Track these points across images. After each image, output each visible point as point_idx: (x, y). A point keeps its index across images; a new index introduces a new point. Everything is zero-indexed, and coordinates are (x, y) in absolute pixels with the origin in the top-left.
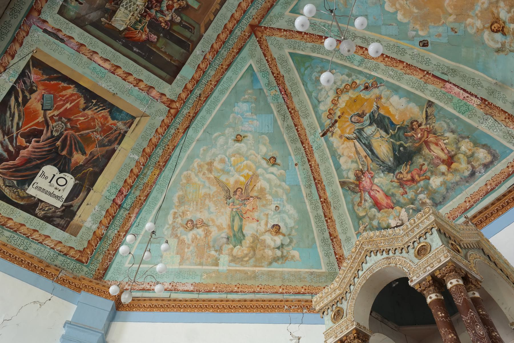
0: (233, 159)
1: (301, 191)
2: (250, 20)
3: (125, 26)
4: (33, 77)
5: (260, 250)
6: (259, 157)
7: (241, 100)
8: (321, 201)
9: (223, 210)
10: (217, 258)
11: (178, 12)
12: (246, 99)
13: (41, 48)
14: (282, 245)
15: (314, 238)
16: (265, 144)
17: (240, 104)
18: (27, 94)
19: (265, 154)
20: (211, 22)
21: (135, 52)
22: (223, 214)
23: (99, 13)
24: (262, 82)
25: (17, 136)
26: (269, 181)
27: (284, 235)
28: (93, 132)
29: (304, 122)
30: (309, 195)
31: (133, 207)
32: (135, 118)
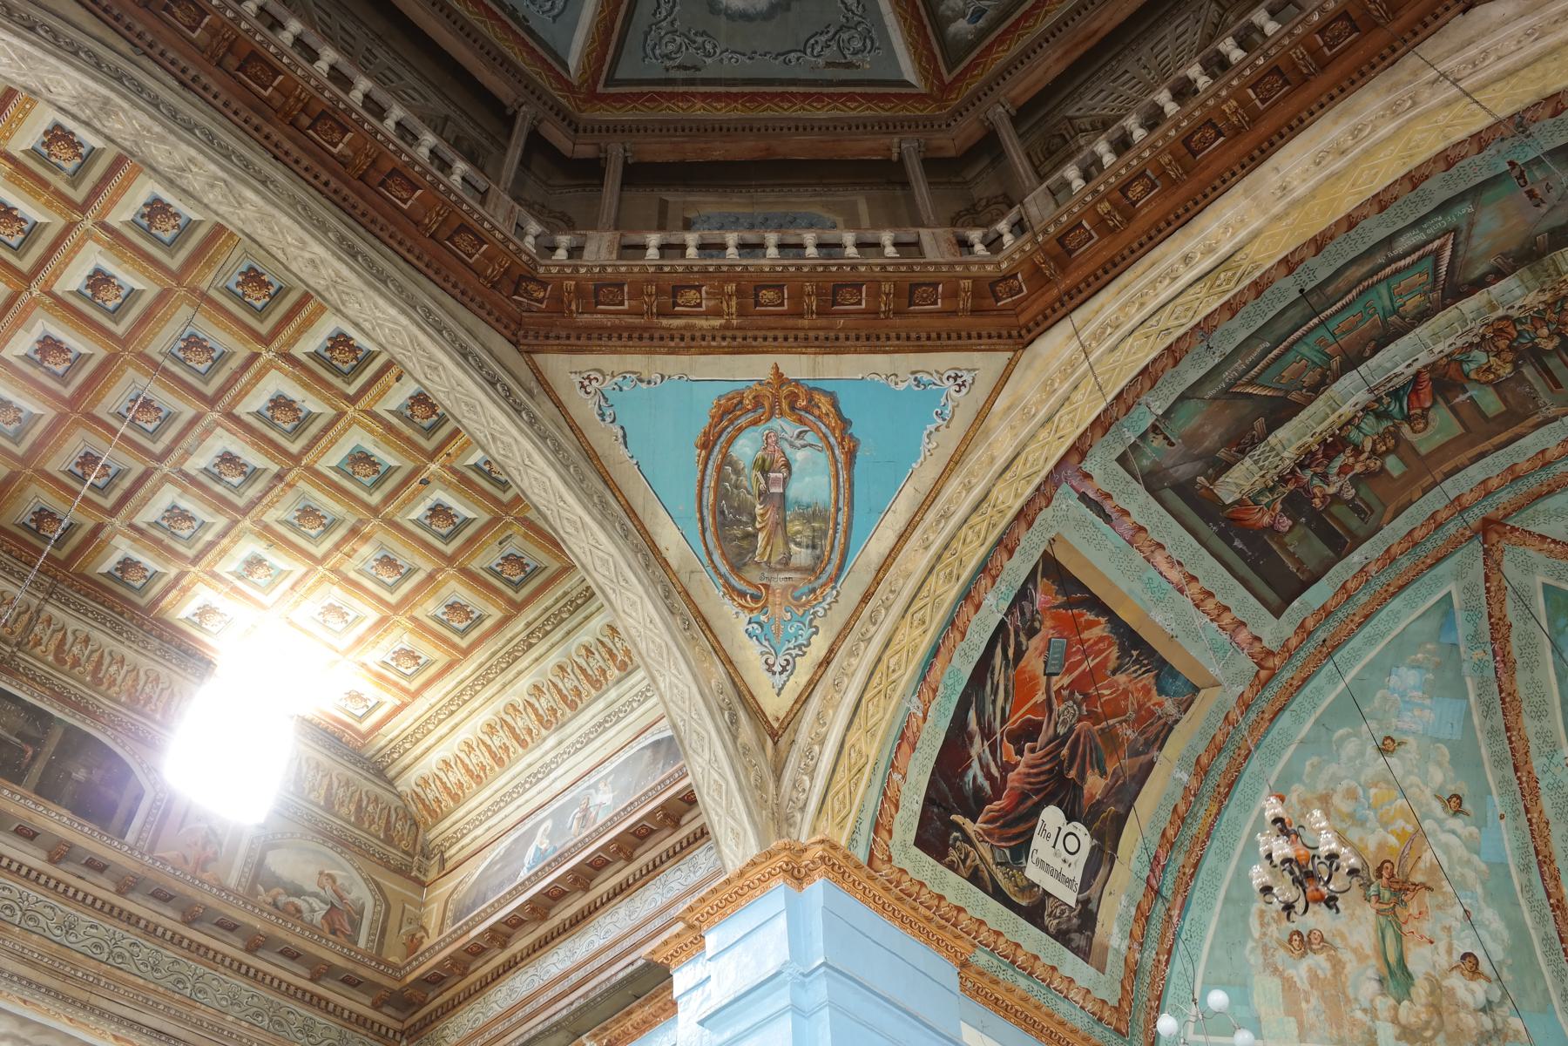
0: (1373, 791)
1: (1510, 877)
2: (1489, 510)
3: (1238, 496)
4: (1039, 598)
5: (1451, 1014)
6: (1428, 792)
7: (1408, 661)
8: (1551, 905)
9: (1358, 912)
10: (1370, 1029)
11: (1356, 480)
12: (1418, 660)
13: (1066, 535)
14: (1489, 1002)
15: (1546, 990)
16: (1440, 765)
17: (1403, 670)
18: (1023, 638)
19: (1441, 787)
20: (1411, 503)
21: (1235, 549)
22: (1360, 923)
23: (1199, 465)
24: (1463, 629)
25: (1002, 740)
26: (1447, 849)
27: (1489, 980)
28: (1120, 723)
29: (1529, 726)
30: (1527, 888)
31: (1176, 893)
32: (1197, 690)
